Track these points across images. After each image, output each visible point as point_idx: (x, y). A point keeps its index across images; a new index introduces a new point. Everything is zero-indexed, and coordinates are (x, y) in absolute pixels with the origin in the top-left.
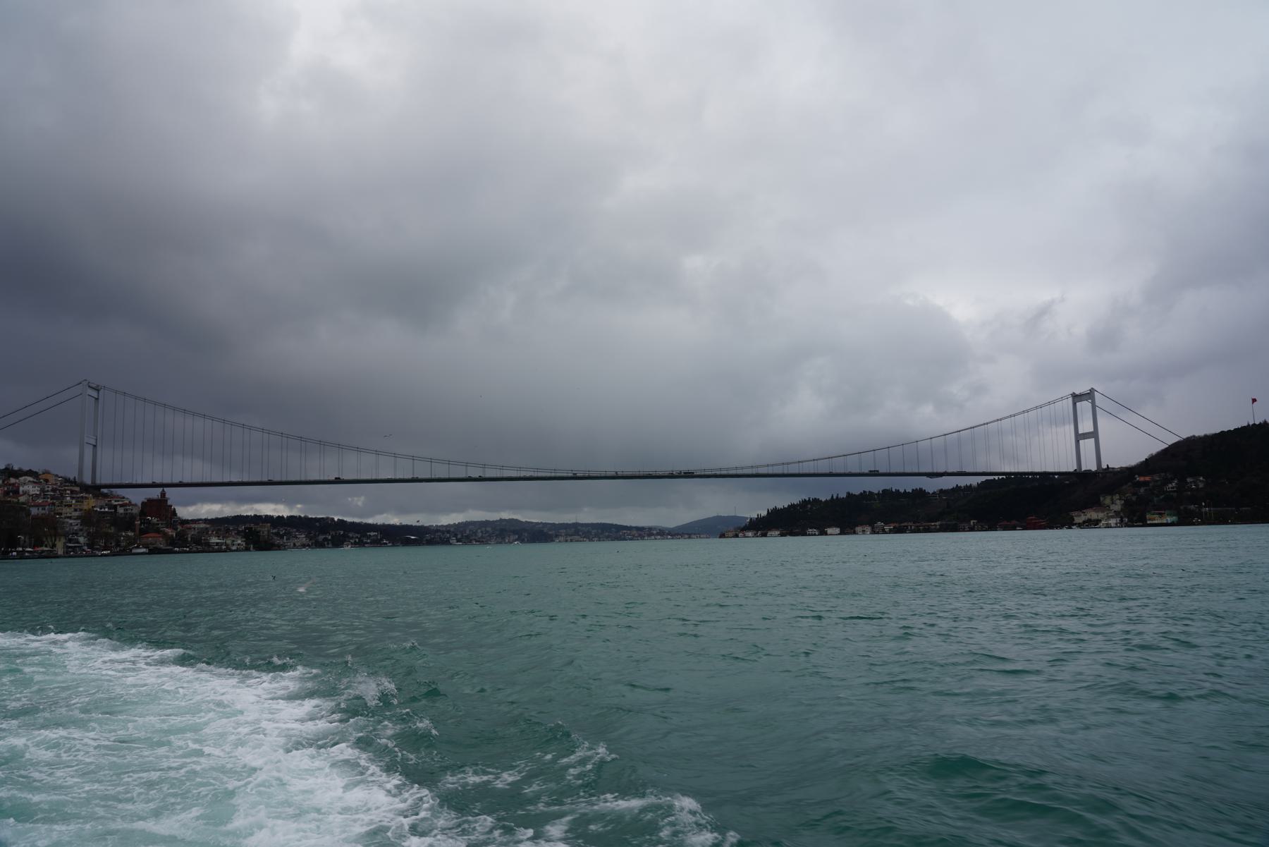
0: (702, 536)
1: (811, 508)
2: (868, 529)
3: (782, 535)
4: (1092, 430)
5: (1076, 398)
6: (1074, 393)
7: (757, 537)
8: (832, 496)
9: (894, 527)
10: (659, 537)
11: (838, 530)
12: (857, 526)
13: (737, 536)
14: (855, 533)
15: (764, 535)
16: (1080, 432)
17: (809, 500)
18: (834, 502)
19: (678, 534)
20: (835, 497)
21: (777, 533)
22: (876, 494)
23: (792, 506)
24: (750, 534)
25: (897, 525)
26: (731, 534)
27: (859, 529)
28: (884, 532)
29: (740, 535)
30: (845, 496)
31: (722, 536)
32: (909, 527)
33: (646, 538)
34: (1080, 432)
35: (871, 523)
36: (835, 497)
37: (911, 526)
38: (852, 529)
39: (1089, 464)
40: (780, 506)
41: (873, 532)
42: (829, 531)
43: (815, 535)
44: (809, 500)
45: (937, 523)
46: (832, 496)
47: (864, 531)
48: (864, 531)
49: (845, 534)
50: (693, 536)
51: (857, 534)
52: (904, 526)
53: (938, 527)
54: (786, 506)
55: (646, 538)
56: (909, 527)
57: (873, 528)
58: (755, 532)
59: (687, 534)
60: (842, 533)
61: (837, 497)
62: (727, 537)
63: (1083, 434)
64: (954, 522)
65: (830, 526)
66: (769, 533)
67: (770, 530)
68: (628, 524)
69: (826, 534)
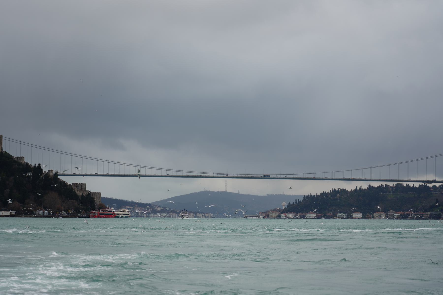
0: (207, 215)
1: (340, 197)
3: (318, 217)
7: (297, 218)
8: (357, 188)
9: (401, 215)
10: (165, 214)
11: (360, 215)
12: (375, 212)
13: (279, 217)
14: (373, 217)
15: (304, 217)
17: (339, 190)
18: (358, 192)
19: (173, 212)
20: (358, 188)
21: (314, 215)
22: (391, 187)
23: (324, 194)
24: (291, 215)
25: (402, 213)
26: (275, 215)
27: (376, 215)
28: (393, 218)
29: (283, 216)
30: (366, 188)
31: (267, 216)
32: (410, 215)
33: (152, 215)
35: (386, 210)
36: (358, 188)
38: (371, 214)
40: (314, 193)
41: (387, 217)
42: (354, 215)
43: (343, 218)
44: (339, 190)
45: (429, 213)
46: (357, 188)
47: (380, 216)
48: (380, 216)
49: (366, 219)
50: (198, 215)
51: (375, 218)
52: (408, 214)
53: (429, 215)
54: (319, 194)
55: (152, 215)
56: (410, 215)
57: (387, 214)
58: (295, 214)
59: (194, 213)
60: (364, 217)
61: (360, 189)
62: (272, 218)
64: (439, 213)
65: (355, 212)
66: (307, 216)
67: (309, 213)
68: (130, 200)
69: (352, 218)
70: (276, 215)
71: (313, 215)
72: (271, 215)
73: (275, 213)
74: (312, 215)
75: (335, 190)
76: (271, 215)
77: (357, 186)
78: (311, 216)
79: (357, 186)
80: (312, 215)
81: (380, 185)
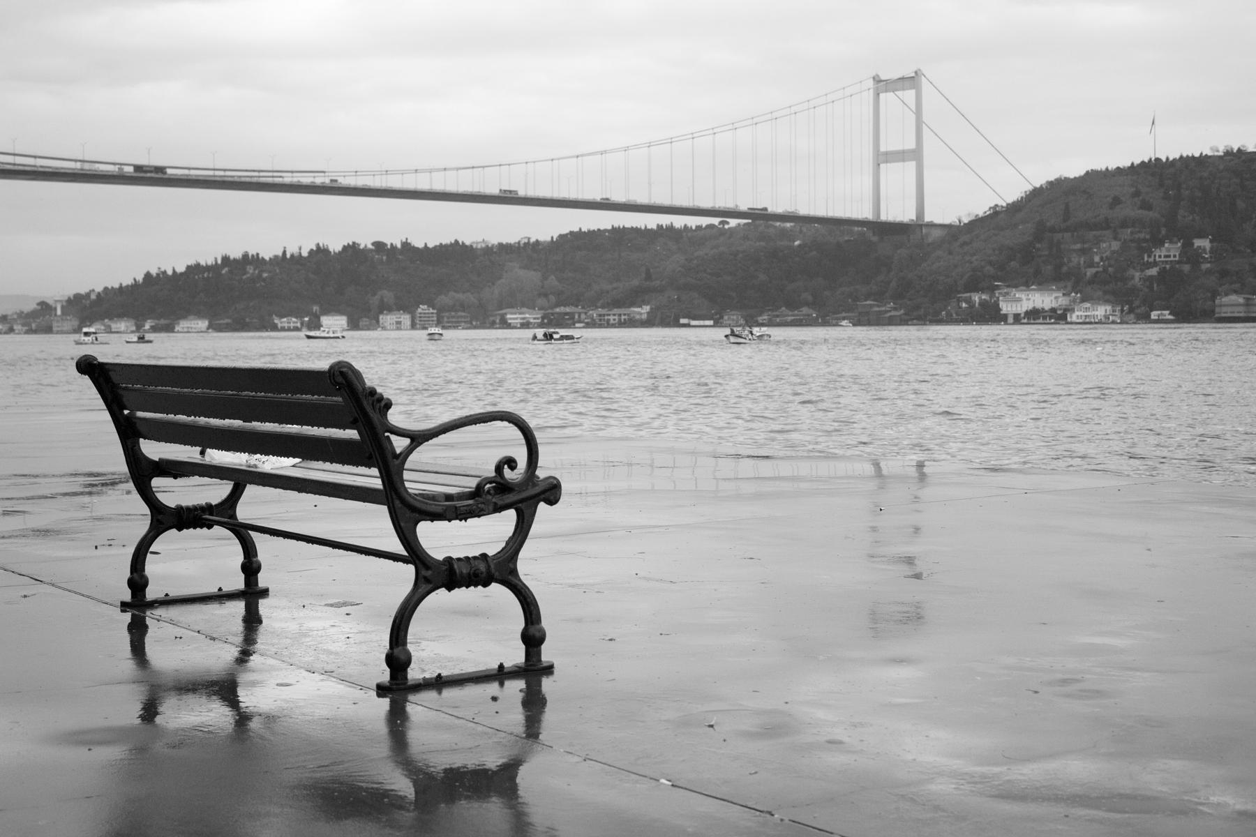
2: (406, 319)
4: (911, 145)
5: (882, 85)
6: (878, 76)
16: (883, 149)
21: (203, 324)
34: (883, 149)
37: (580, 314)
39: (898, 210)
52: (567, 314)
56: (577, 317)
60: (354, 325)
62: (58, 333)
63: (886, 153)
67: (184, 317)
70: (73, 326)
71: (200, 322)
72: (58, 327)
73: (71, 320)
74: (198, 324)
75: (229, 257)
76: (58, 327)
77: (285, 248)
78: (193, 326)
79: (285, 248)
80: (196, 322)
81: (351, 243)
